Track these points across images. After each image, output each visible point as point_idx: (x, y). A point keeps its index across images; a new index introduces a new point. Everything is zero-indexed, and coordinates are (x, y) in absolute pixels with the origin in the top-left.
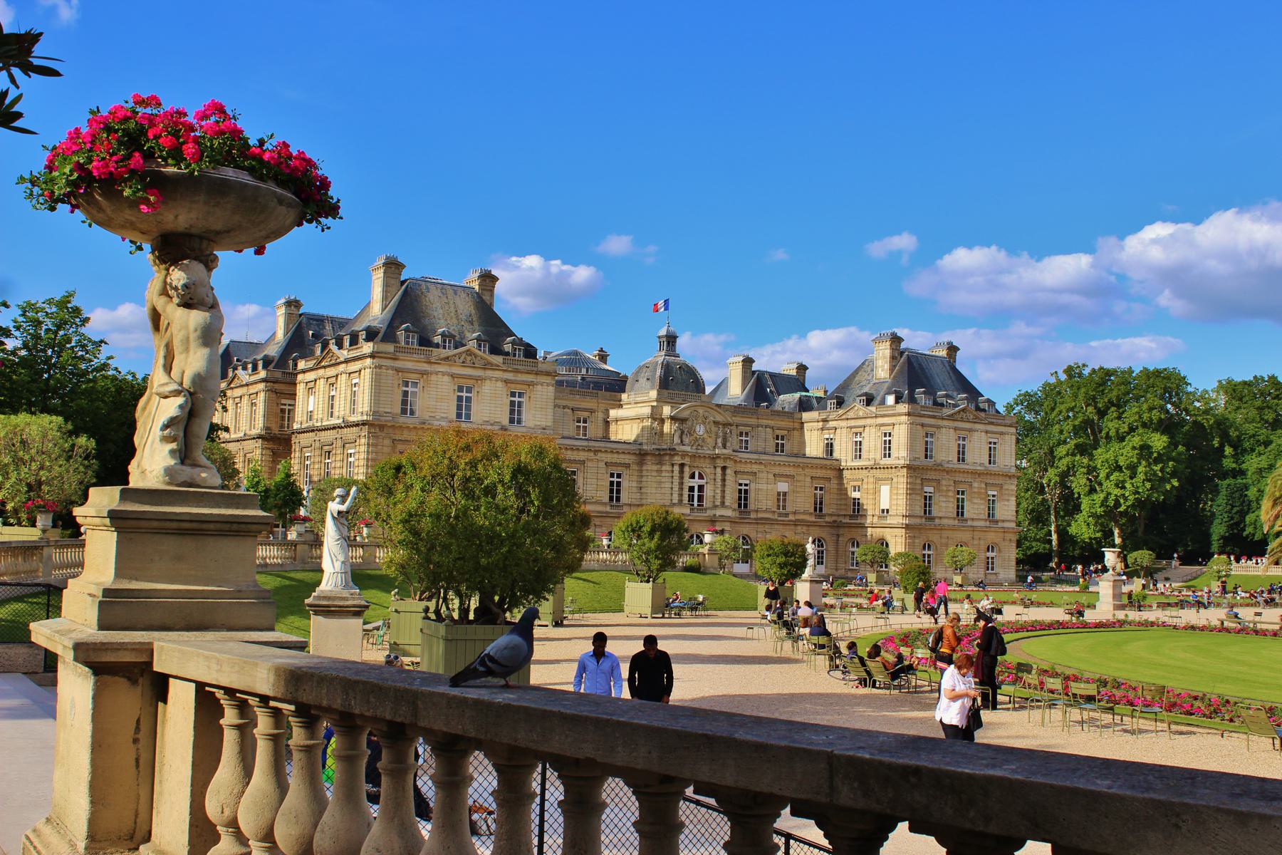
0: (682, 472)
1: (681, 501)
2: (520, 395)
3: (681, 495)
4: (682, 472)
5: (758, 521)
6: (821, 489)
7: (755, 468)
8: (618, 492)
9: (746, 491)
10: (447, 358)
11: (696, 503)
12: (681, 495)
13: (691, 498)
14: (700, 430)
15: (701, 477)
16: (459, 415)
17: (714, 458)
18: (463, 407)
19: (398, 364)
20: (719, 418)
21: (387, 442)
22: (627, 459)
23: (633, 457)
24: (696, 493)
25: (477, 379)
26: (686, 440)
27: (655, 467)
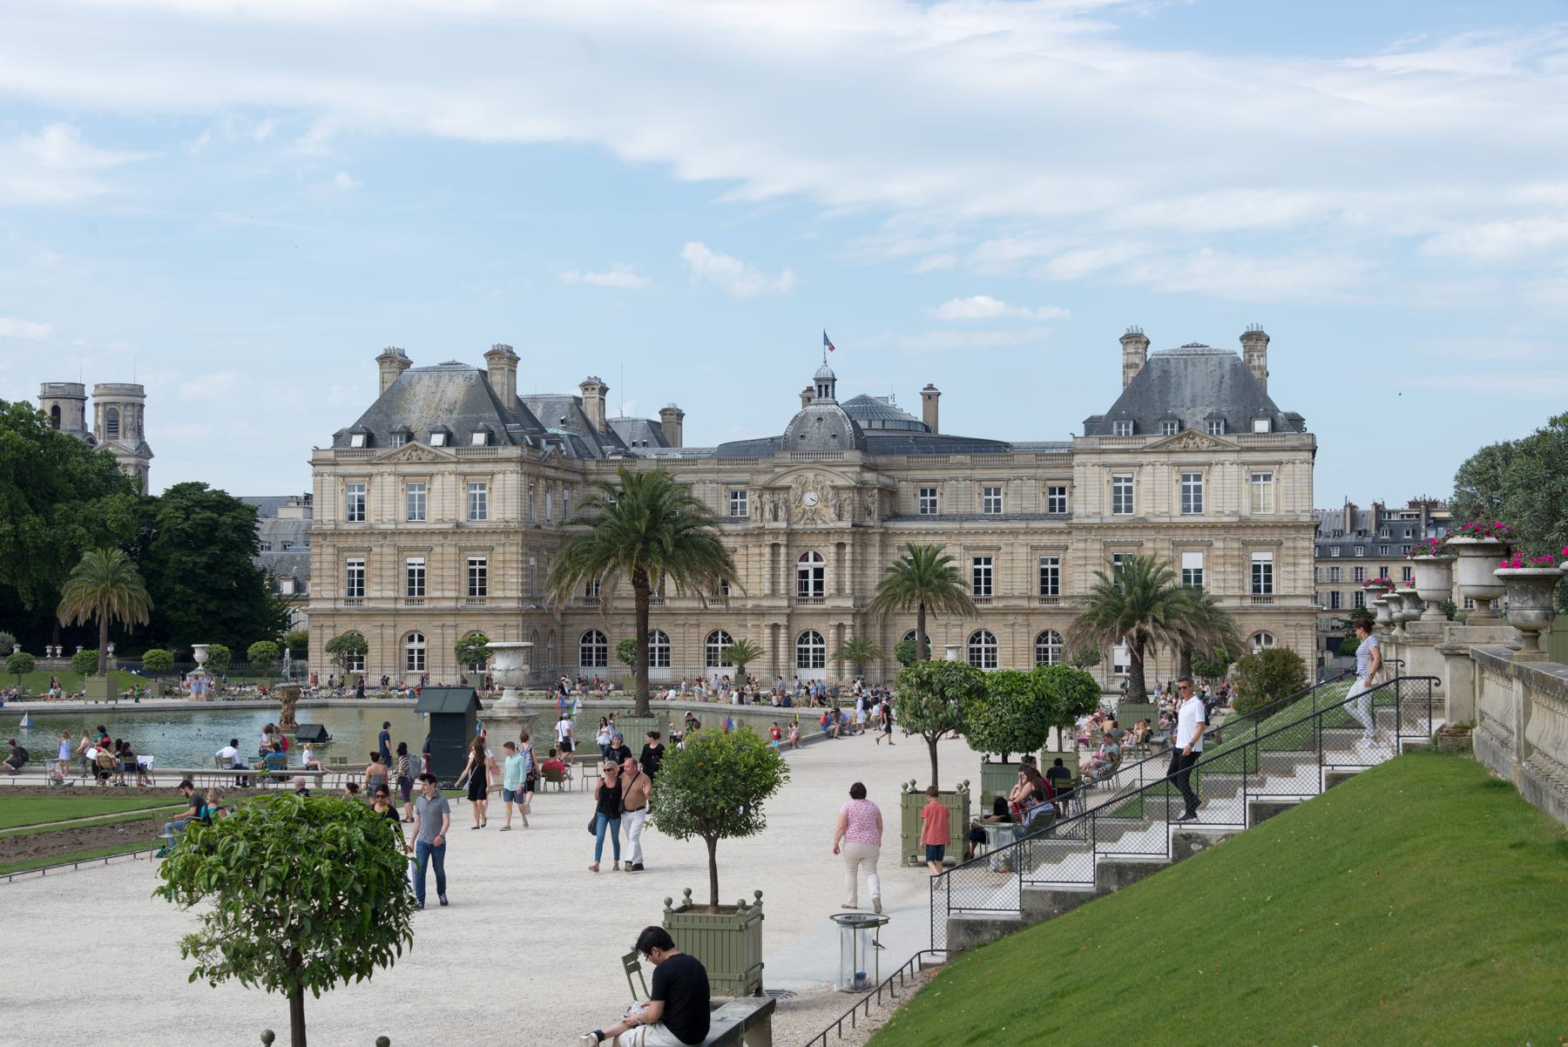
1: (774, 593)
2: (482, 487)
3: (774, 582)
6: (1055, 561)
10: (390, 457)
11: (811, 592)
14: (810, 498)
15: (817, 558)
16: (411, 517)
17: (828, 533)
19: (340, 470)
20: (840, 482)
21: (330, 550)
23: (740, 539)
24: (811, 580)
25: (425, 475)
26: (781, 514)
27: (757, 550)
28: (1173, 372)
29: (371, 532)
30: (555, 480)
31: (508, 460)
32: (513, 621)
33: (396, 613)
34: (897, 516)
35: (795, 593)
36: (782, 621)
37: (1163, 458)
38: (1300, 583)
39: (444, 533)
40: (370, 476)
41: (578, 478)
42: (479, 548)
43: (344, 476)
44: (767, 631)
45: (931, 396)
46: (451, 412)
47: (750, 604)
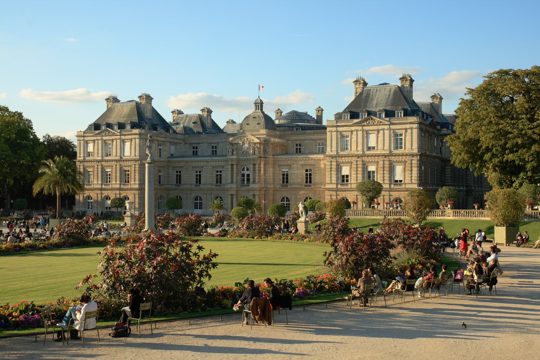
0: (232, 168)
1: (232, 182)
3: (232, 179)
4: (232, 168)
7: (289, 162)
8: (221, 179)
9: (287, 175)
10: (99, 134)
12: (232, 179)
15: (247, 170)
19: (86, 139)
22: (222, 164)
23: (225, 163)
24: (246, 177)
26: (234, 153)
28: (371, 94)
30: (164, 142)
31: (136, 134)
32: (137, 192)
33: (102, 189)
34: (287, 154)
35: (240, 182)
36: (234, 193)
37: (360, 128)
38: (413, 178)
41: (181, 141)
42: (127, 166)
44: (229, 196)
45: (320, 110)
46: (124, 118)
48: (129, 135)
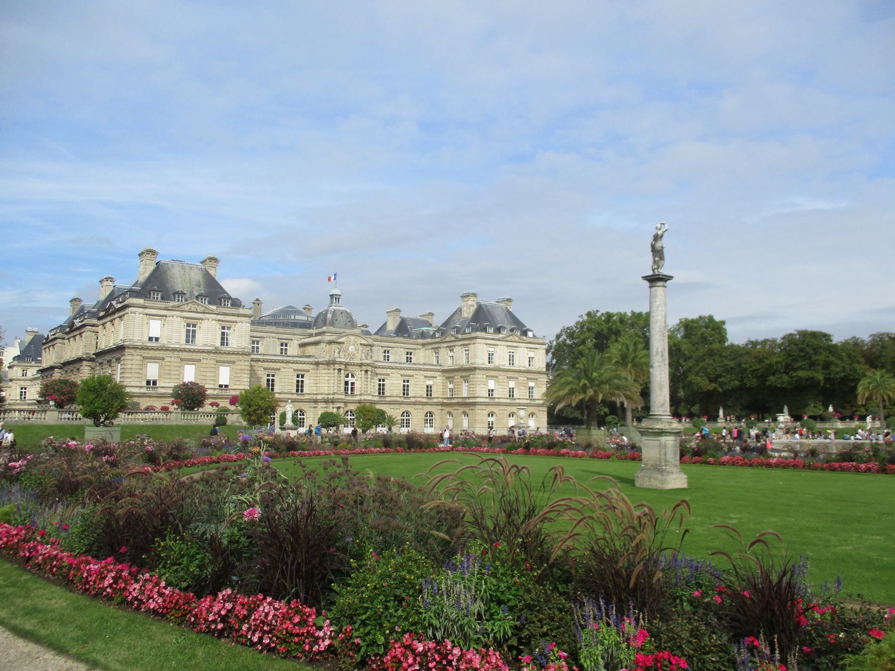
5: (390, 403)
8: (302, 386)
11: (349, 392)
13: (346, 389)
14: (351, 348)
15: (353, 376)
16: (187, 341)
17: (361, 365)
18: (191, 336)
20: (364, 342)
21: (139, 358)
24: (350, 386)
25: (199, 319)
26: (342, 355)
29: (166, 349)
31: (245, 316)
37: (504, 343)
39: (209, 352)
40: (166, 316)
43: (150, 315)
47: (319, 397)
48: (233, 315)
